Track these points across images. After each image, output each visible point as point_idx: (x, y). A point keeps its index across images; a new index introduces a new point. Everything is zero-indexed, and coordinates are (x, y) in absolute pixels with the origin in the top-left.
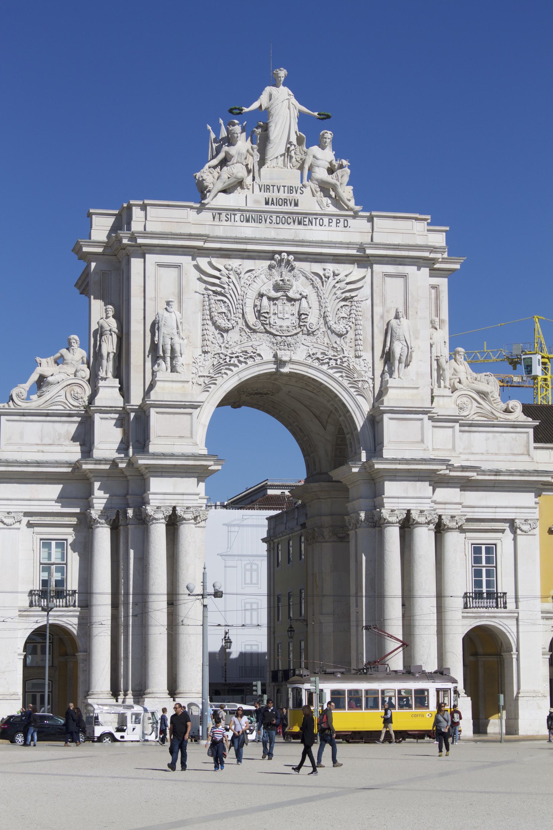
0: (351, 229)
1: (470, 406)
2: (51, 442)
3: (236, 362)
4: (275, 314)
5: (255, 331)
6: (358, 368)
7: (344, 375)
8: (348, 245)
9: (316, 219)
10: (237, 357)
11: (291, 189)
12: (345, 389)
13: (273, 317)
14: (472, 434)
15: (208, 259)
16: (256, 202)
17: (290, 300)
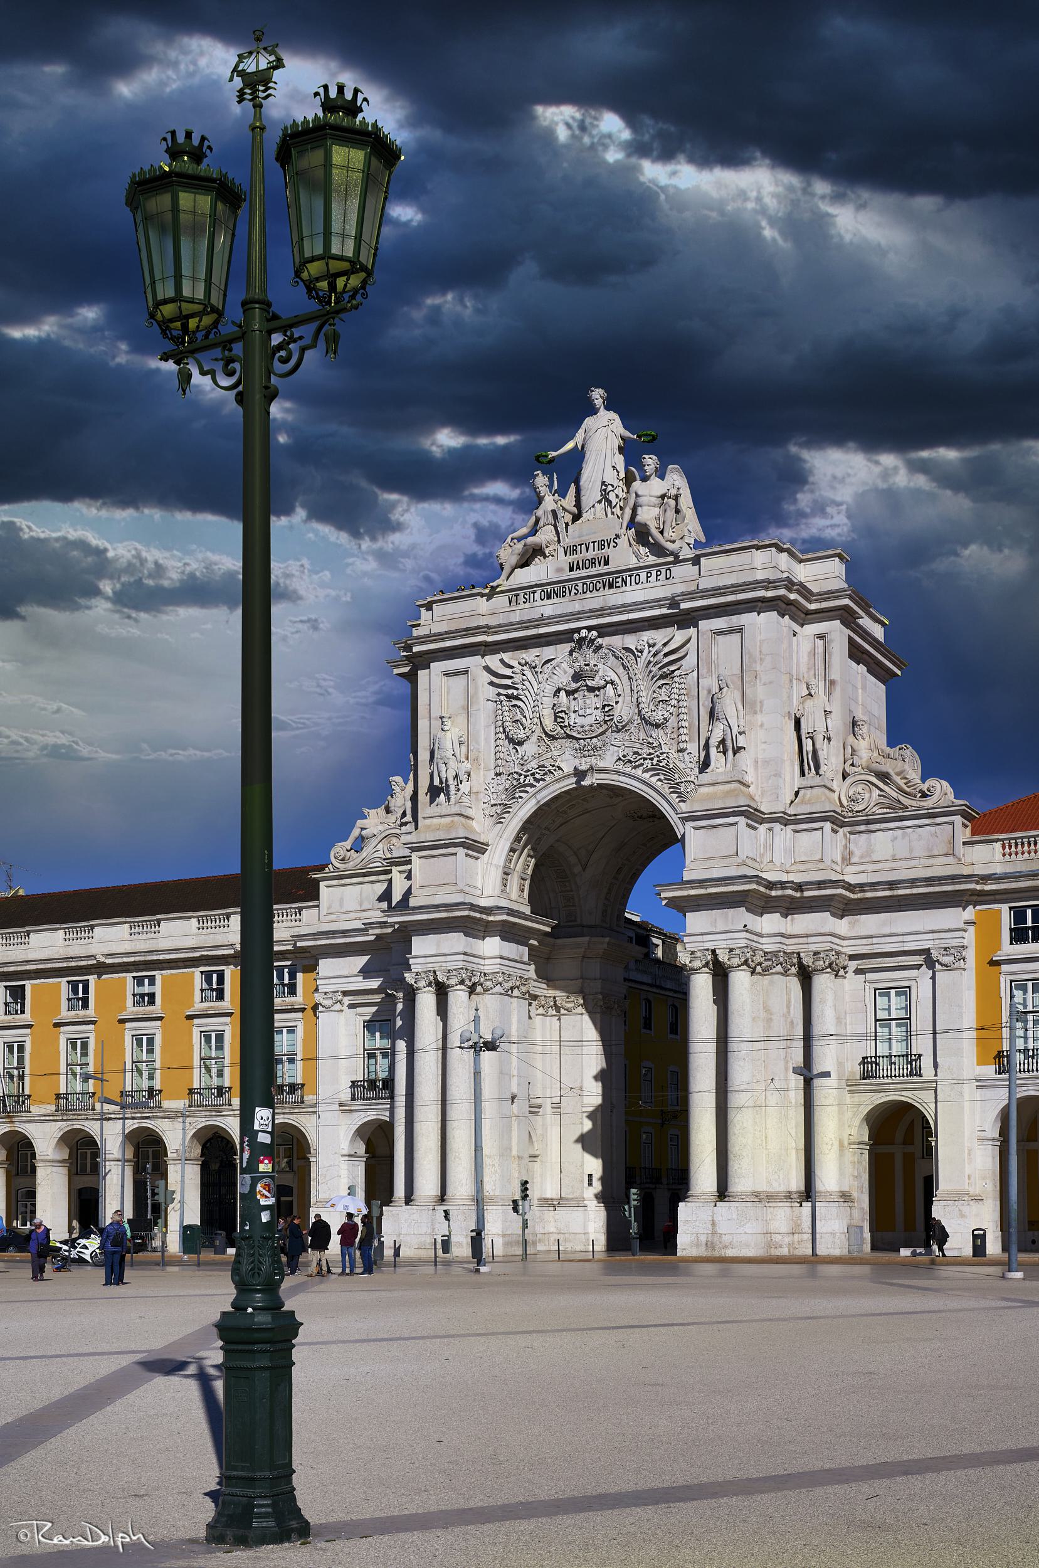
0: (675, 581)
1: (867, 795)
2: (370, 907)
3: (532, 781)
4: (575, 712)
5: (553, 738)
6: (681, 765)
7: (662, 777)
8: (657, 603)
9: (631, 576)
10: (533, 774)
11: (602, 544)
12: (664, 797)
13: (573, 715)
14: (873, 835)
15: (498, 657)
16: (559, 570)
17: (591, 689)
